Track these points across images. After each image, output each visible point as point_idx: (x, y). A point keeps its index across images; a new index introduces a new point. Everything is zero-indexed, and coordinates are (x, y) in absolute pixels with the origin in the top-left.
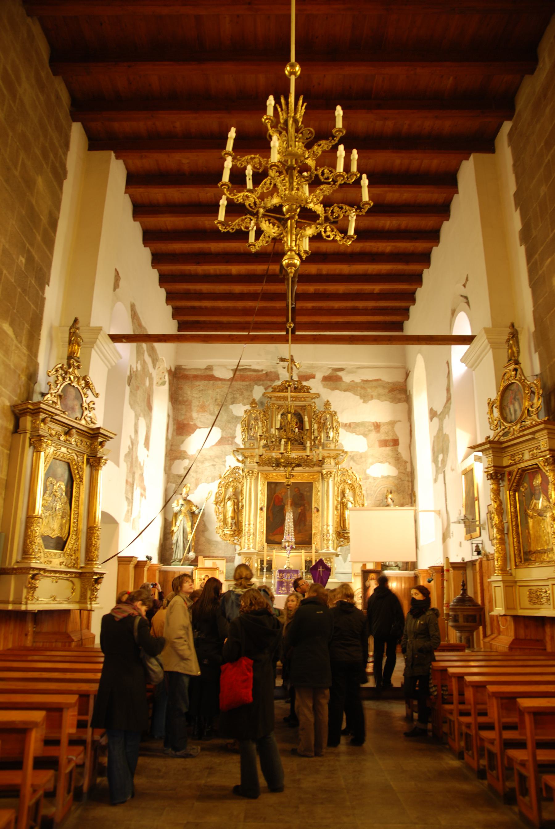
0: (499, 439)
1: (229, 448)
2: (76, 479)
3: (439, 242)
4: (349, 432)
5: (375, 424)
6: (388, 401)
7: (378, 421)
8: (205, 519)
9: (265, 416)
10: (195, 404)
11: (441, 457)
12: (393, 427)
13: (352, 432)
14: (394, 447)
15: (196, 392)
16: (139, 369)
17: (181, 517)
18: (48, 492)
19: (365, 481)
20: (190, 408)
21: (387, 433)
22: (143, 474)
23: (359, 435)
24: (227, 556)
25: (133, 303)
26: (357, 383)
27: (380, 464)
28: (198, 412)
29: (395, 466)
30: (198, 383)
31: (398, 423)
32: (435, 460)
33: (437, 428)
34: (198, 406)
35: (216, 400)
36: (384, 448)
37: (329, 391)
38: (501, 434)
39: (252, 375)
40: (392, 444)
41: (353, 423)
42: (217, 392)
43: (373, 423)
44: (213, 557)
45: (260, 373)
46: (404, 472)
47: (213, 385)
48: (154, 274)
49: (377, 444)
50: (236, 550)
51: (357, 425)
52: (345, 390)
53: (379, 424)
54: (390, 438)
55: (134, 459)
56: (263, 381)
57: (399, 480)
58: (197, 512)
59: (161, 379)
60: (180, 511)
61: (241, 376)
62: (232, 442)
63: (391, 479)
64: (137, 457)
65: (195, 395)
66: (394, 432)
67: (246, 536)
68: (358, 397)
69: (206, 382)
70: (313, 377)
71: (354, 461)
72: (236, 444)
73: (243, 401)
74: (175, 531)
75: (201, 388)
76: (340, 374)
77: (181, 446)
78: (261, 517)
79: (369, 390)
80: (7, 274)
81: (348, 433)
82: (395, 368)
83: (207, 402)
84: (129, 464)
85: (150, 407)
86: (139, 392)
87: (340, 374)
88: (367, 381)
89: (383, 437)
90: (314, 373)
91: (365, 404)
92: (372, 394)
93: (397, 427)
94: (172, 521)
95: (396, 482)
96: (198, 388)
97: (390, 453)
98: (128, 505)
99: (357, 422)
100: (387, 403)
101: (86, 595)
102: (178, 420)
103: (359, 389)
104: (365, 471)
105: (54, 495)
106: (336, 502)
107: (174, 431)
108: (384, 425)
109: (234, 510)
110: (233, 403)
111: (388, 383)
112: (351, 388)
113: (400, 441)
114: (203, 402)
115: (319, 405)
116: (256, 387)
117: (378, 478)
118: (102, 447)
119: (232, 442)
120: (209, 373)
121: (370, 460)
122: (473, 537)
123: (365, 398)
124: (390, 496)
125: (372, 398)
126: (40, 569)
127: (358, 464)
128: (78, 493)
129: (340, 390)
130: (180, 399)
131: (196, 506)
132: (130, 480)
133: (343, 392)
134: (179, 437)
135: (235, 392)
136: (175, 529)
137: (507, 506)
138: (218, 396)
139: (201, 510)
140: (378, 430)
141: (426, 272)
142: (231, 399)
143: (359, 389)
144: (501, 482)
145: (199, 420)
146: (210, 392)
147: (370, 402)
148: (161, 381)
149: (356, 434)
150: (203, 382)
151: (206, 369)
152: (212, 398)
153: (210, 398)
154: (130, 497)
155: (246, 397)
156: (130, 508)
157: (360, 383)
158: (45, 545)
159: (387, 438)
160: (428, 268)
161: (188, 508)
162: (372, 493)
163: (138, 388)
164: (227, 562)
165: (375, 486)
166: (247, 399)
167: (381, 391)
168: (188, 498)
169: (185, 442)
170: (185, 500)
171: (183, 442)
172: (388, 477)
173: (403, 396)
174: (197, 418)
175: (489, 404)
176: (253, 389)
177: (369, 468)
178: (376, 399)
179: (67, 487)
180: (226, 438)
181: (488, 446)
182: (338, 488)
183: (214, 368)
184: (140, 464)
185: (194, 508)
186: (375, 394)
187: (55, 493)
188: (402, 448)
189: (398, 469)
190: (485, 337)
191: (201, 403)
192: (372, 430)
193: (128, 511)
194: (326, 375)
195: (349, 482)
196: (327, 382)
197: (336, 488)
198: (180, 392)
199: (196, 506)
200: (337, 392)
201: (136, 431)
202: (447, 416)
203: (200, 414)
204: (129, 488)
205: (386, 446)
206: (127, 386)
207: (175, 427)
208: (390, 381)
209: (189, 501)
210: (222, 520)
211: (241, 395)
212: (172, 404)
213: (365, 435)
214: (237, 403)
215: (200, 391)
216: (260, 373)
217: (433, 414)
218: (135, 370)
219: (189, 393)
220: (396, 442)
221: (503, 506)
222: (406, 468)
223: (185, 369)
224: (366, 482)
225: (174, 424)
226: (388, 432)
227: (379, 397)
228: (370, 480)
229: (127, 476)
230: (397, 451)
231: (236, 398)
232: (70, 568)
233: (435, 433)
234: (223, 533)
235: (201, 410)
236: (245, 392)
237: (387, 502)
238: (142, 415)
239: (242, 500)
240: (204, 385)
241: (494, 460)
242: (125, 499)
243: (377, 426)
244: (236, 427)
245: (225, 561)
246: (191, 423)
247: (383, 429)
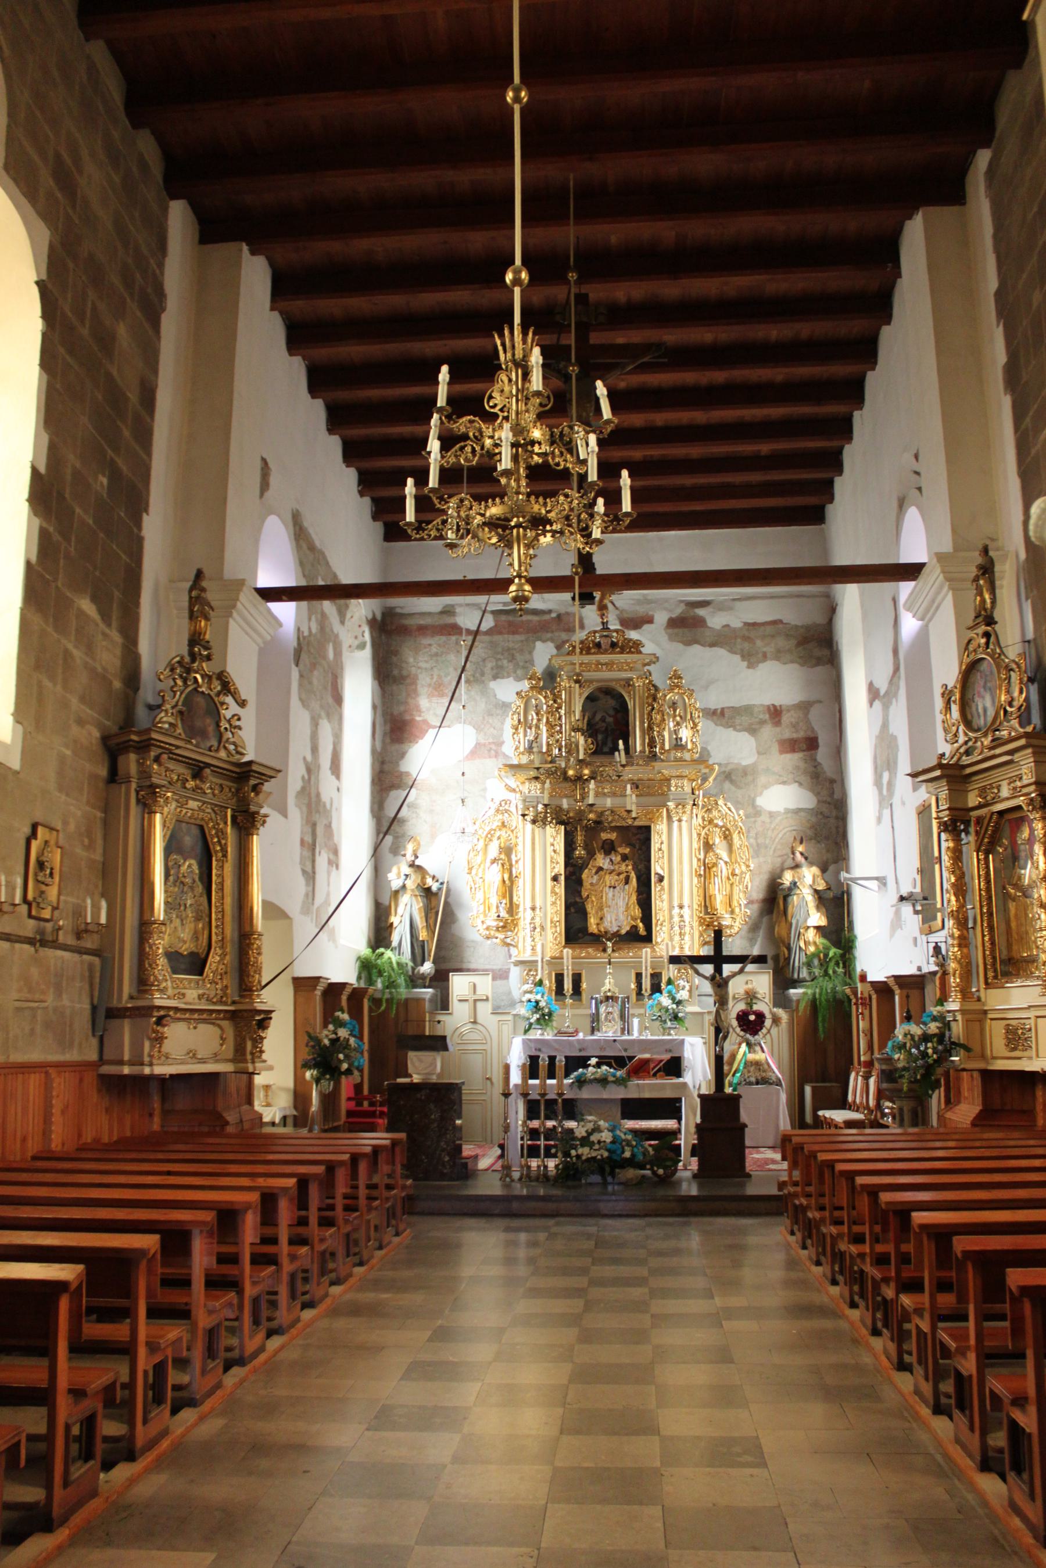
0: (959, 759)
1: (492, 765)
2: (216, 852)
3: (875, 363)
4: (721, 725)
6: (796, 662)
7: (777, 704)
8: (450, 900)
9: (555, 701)
10: (424, 682)
11: (886, 776)
12: (806, 714)
13: (727, 726)
14: (809, 753)
16: (314, 631)
17: (405, 899)
18: (171, 878)
19: (753, 819)
20: (415, 691)
21: (794, 726)
22: (330, 823)
23: (739, 731)
24: (495, 967)
25: (297, 511)
26: (734, 630)
27: (781, 786)
28: (430, 696)
29: (812, 790)
30: (426, 641)
31: (817, 706)
32: (878, 782)
33: (880, 723)
34: (430, 685)
36: (789, 756)
37: (681, 646)
38: (962, 750)
39: (531, 621)
40: (804, 747)
41: (729, 708)
43: (768, 707)
44: (468, 970)
45: (547, 617)
46: (829, 800)
48: (334, 444)
49: (775, 748)
50: (510, 956)
51: (737, 711)
52: (712, 645)
54: (801, 734)
55: (314, 799)
56: (552, 632)
57: (820, 817)
58: (434, 889)
59: (356, 637)
60: (404, 887)
61: (510, 624)
62: (497, 752)
63: (802, 814)
64: (318, 795)
65: (423, 665)
66: (808, 722)
67: (528, 931)
68: (737, 658)
69: (443, 638)
70: (650, 620)
71: (732, 782)
72: (505, 755)
73: (515, 672)
74: (395, 925)
75: (434, 649)
76: (701, 612)
77: (401, 763)
78: (553, 892)
79: (759, 643)
80: (81, 513)
81: (720, 729)
82: (808, 597)
84: (305, 809)
85: (338, 699)
86: (316, 673)
87: (701, 612)
88: (754, 624)
89: (788, 734)
90: (651, 613)
91: (751, 671)
92: (765, 649)
93: (815, 714)
94: (390, 906)
95: (814, 819)
97: (802, 765)
98: (307, 885)
100: (794, 667)
101: (244, 1049)
102: (392, 714)
103: (739, 640)
104: (754, 800)
105: (182, 882)
106: (695, 861)
107: (385, 735)
108: (788, 711)
109: (504, 881)
110: (495, 677)
111: (796, 626)
112: (724, 639)
113: (821, 741)
114: (440, 677)
115: (659, 678)
116: (539, 644)
117: (778, 813)
118: (257, 794)
119: (497, 752)
120: (450, 620)
121: (762, 779)
122: (933, 930)
123: (752, 659)
124: (801, 848)
125: (765, 657)
126: (169, 1008)
127: (738, 787)
128: (221, 876)
129: (702, 645)
130: (396, 672)
131: (434, 877)
132: (308, 839)
133: (708, 648)
134: (396, 746)
135: (499, 656)
136: (394, 920)
137: (972, 878)
139: (442, 884)
141: (857, 414)
142: (492, 669)
143: (739, 640)
144: (963, 835)
145: (431, 712)
147: (761, 665)
148: (356, 642)
149: (735, 729)
150: (437, 638)
151: (442, 613)
153: (451, 669)
154: (309, 869)
155: (521, 664)
156: (310, 889)
157: (741, 629)
158: (172, 968)
159: (795, 736)
160: (861, 409)
161: (419, 881)
162: (767, 842)
163: (314, 666)
164: (494, 979)
165: (773, 830)
166: (524, 667)
167: (781, 642)
168: (417, 863)
169: (408, 755)
170: (412, 865)
171: (403, 755)
172: (797, 811)
173: (826, 652)
174: (428, 710)
175: (943, 694)
176: (534, 647)
177: (761, 794)
178: (771, 659)
179: (200, 867)
180: (484, 745)
181: (938, 773)
182: (699, 835)
183: (458, 610)
184: (325, 806)
185: (429, 882)
186: (770, 649)
187: (183, 879)
188: (822, 754)
189: (817, 794)
190: (938, 570)
193: (307, 895)
194: (674, 616)
195: (721, 824)
196: (676, 630)
197: (695, 836)
198: (394, 659)
199: (434, 877)
200: (696, 648)
201: (315, 749)
202: (894, 700)
203: (434, 699)
204: (307, 853)
205: (793, 750)
206: (293, 666)
207: (388, 727)
208: (799, 624)
209: (419, 868)
210: (482, 901)
211: (511, 661)
213: (752, 731)
214: (503, 678)
215: (432, 656)
216: (547, 617)
217: (874, 694)
218: (306, 634)
219: (411, 660)
220: (811, 744)
221: (967, 878)
222: (833, 793)
223: (402, 615)
224: (755, 822)
225: (385, 722)
226: (797, 723)
227: (778, 656)
228: (764, 818)
229: (302, 832)
230: (815, 760)
231: (501, 667)
232: (214, 1003)
233: (876, 731)
234: (485, 926)
236: (518, 657)
237: (793, 859)
238: (323, 714)
239: (517, 862)
240: (439, 645)
241: (951, 798)
242: (300, 873)
243: (775, 713)
244: (503, 724)
245: (490, 977)
246: (418, 718)
247: (786, 719)
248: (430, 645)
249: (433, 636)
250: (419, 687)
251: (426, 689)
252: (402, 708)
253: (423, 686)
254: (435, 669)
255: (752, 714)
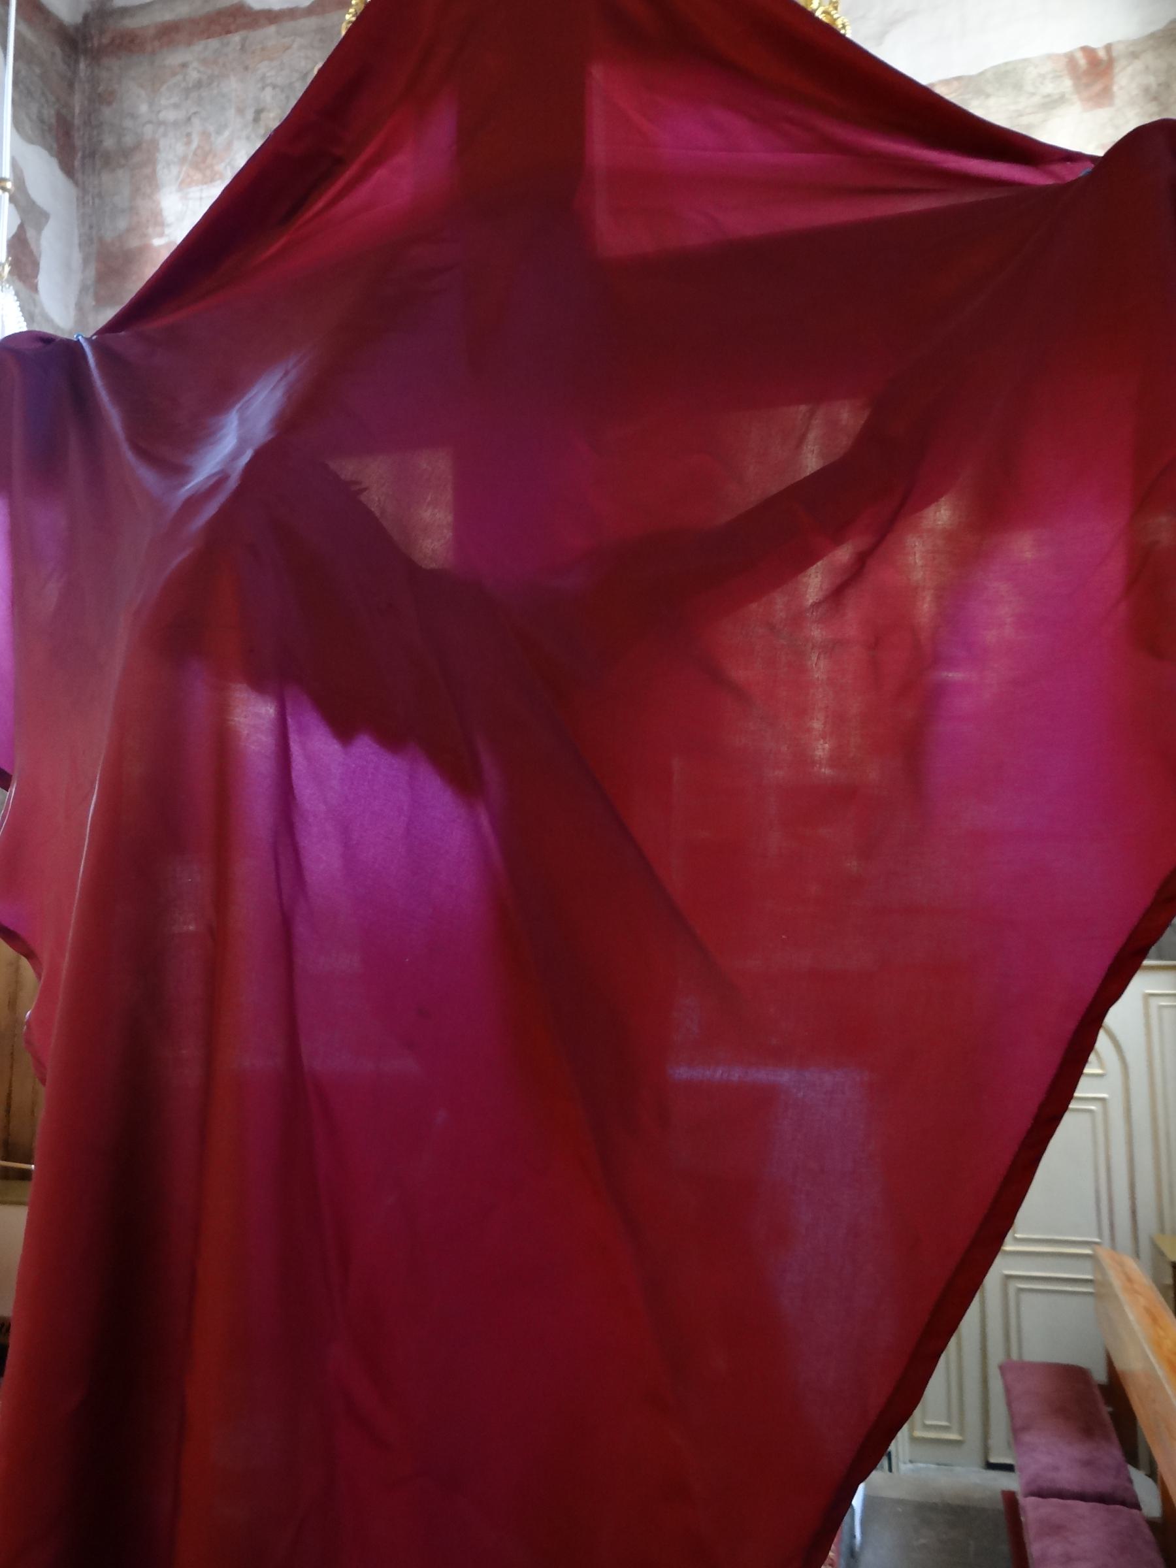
5: (1082, 62)
7: (1097, 43)
15: (175, 99)
30: (174, 58)
34: (183, 160)
35: (258, 113)
42: (263, 78)
43: (1071, 59)
47: (243, 48)
53: (1102, 54)
65: (170, 115)
69: (214, 43)
75: (193, 75)
83: (219, 132)
96: (179, 77)
99: (973, 71)
102: (101, 240)
114: (205, 135)
130: (109, 143)
138: (268, 94)
140: (1098, 87)
146: (233, 85)
152: (241, 111)
153: (231, 113)
191: (194, 145)
192: (1061, 100)
198: (107, 112)
207: (91, 272)
212: (68, 169)
215: (187, 91)
219: (144, 108)
235: (198, 176)
240: (204, 62)
248: (184, 65)
249: (189, 44)
250: (159, 167)
251: (175, 170)
252: (122, 224)
253: (168, 164)
254: (196, 121)
255: (1018, 87)
